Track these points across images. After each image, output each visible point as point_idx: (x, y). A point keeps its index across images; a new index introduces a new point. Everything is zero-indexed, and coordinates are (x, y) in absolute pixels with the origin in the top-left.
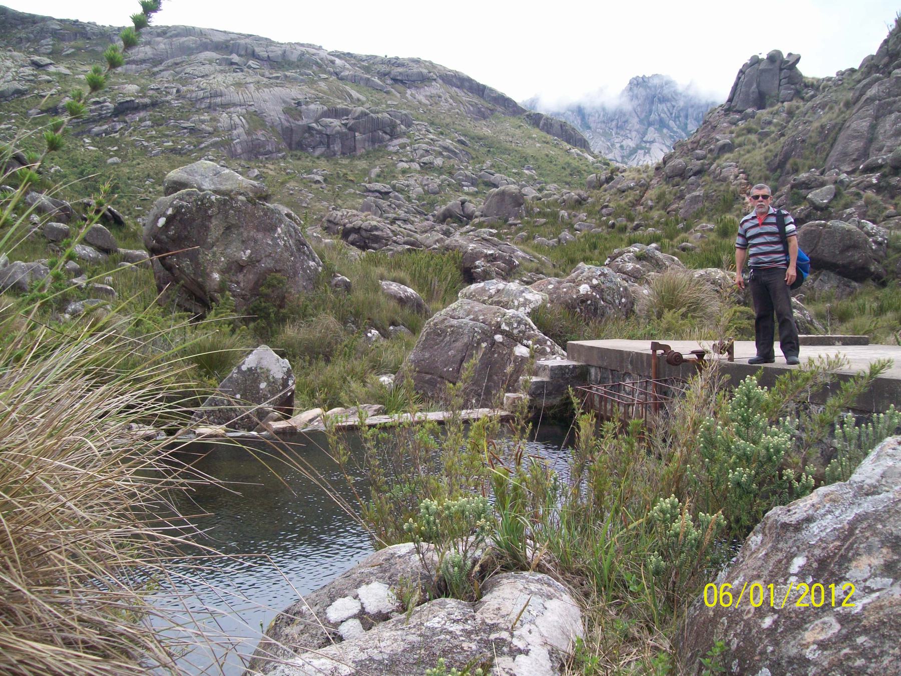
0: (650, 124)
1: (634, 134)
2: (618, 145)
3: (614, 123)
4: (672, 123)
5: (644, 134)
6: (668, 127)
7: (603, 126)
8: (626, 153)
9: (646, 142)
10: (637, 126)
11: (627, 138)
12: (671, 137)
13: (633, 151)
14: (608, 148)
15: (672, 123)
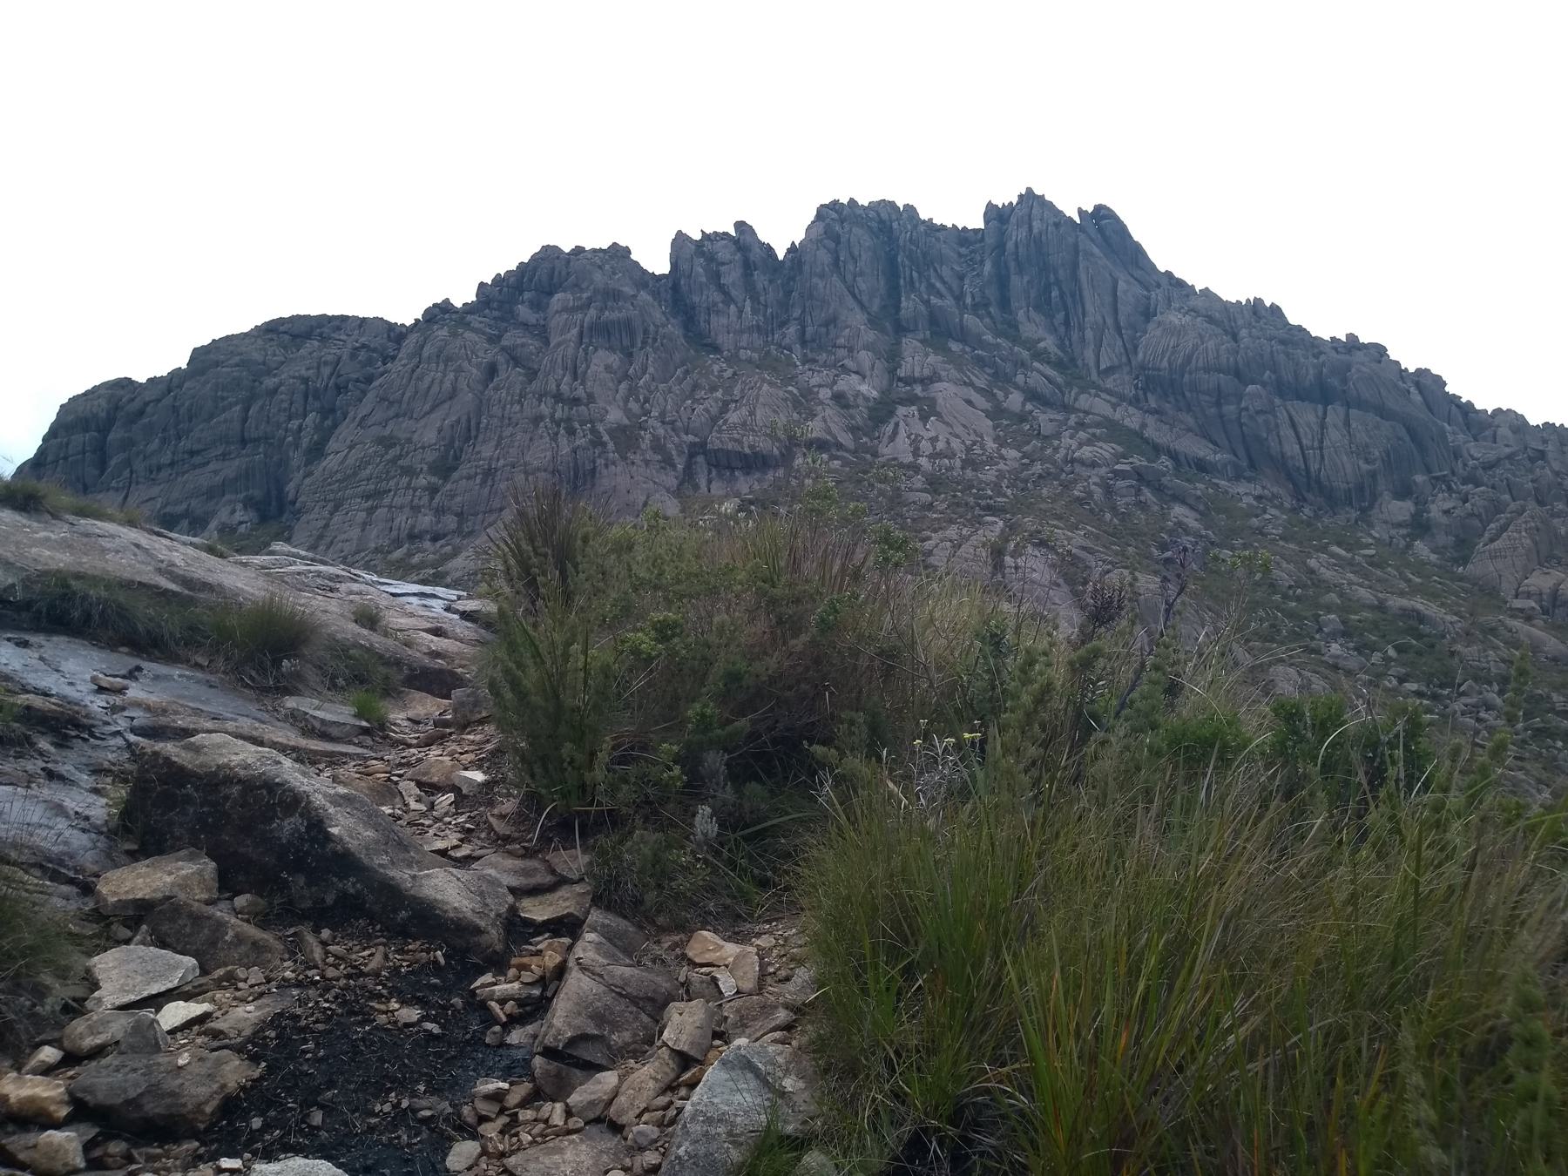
0: (901, 329)
1: (865, 357)
2: (825, 394)
3: (792, 330)
4: (969, 319)
5: (893, 358)
6: (963, 336)
7: (758, 341)
8: (860, 416)
9: (909, 381)
10: (870, 336)
11: (846, 370)
12: (981, 362)
13: (882, 412)
14: (797, 404)
15: (969, 319)
